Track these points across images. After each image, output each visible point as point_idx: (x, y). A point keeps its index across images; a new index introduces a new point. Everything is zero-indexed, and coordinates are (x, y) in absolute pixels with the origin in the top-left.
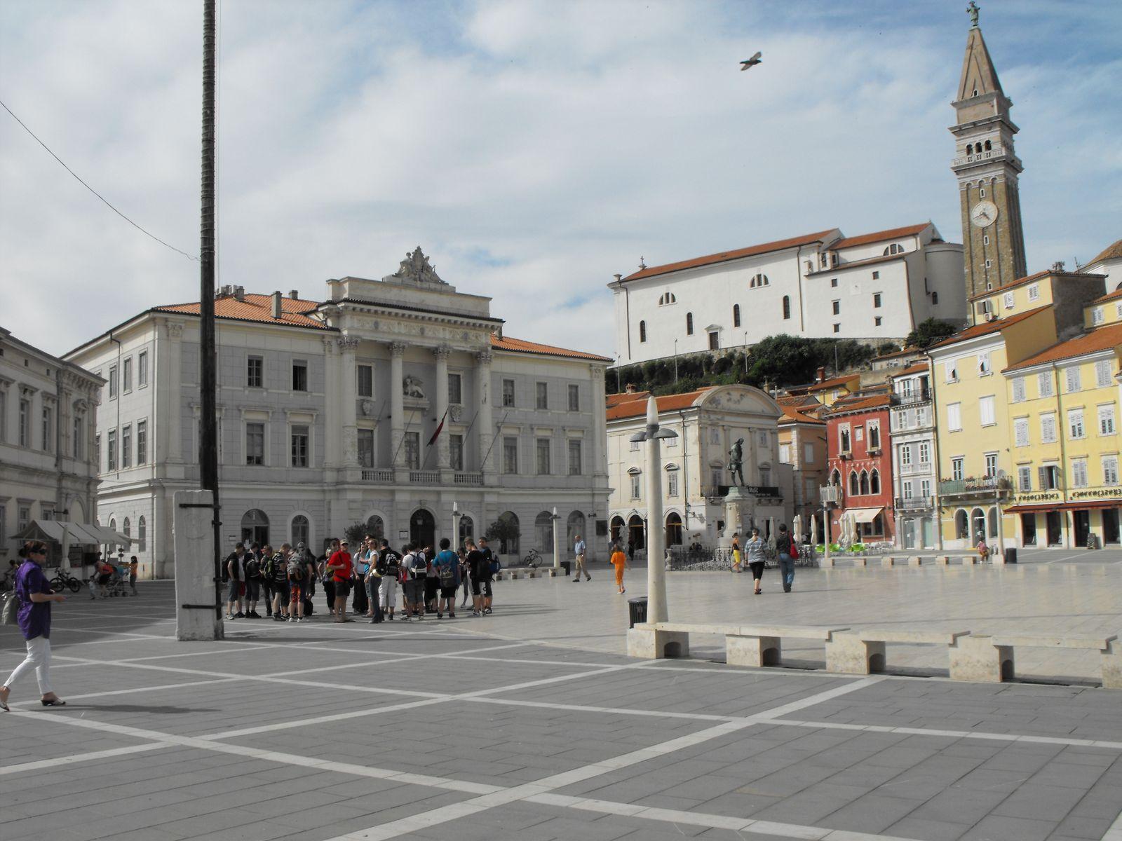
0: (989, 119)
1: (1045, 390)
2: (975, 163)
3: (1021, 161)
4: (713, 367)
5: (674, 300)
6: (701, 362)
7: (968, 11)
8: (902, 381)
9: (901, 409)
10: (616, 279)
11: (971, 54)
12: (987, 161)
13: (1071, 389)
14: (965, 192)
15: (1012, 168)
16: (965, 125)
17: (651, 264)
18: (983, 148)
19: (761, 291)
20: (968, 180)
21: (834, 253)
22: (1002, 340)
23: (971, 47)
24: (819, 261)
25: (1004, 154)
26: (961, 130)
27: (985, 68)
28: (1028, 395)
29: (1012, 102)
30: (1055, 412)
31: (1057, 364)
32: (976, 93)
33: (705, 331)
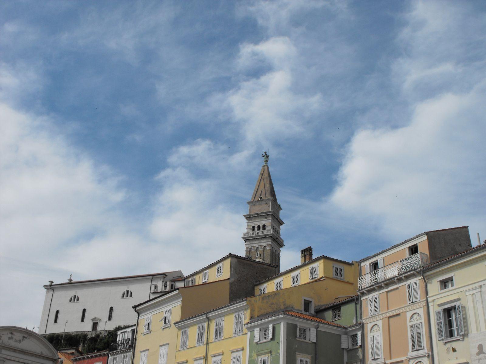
0: (266, 213)
1: (200, 339)
2: (256, 236)
3: (283, 241)
4: (86, 342)
5: (78, 300)
6: (80, 338)
7: (263, 156)
8: (121, 333)
9: (114, 355)
10: (49, 283)
11: (261, 178)
12: (262, 236)
13: (216, 338)
14: (249, 253)
15: (277, 243)
16: (253, 214)
17: (74, 280)
18: (261, 229)
19: (125, 300)
20: (251, 246)
21: (173, 283)
22: (178, 298)
23: (262, 175)
24: (162, 286)
25: (272, 233)
26: (250, 217)
27: (268, 186)
28: (189, 344)
29: (281, 207)
30: (204, 358)
31: (210, 315)
32: (261, 198)
33: (91, 321)
